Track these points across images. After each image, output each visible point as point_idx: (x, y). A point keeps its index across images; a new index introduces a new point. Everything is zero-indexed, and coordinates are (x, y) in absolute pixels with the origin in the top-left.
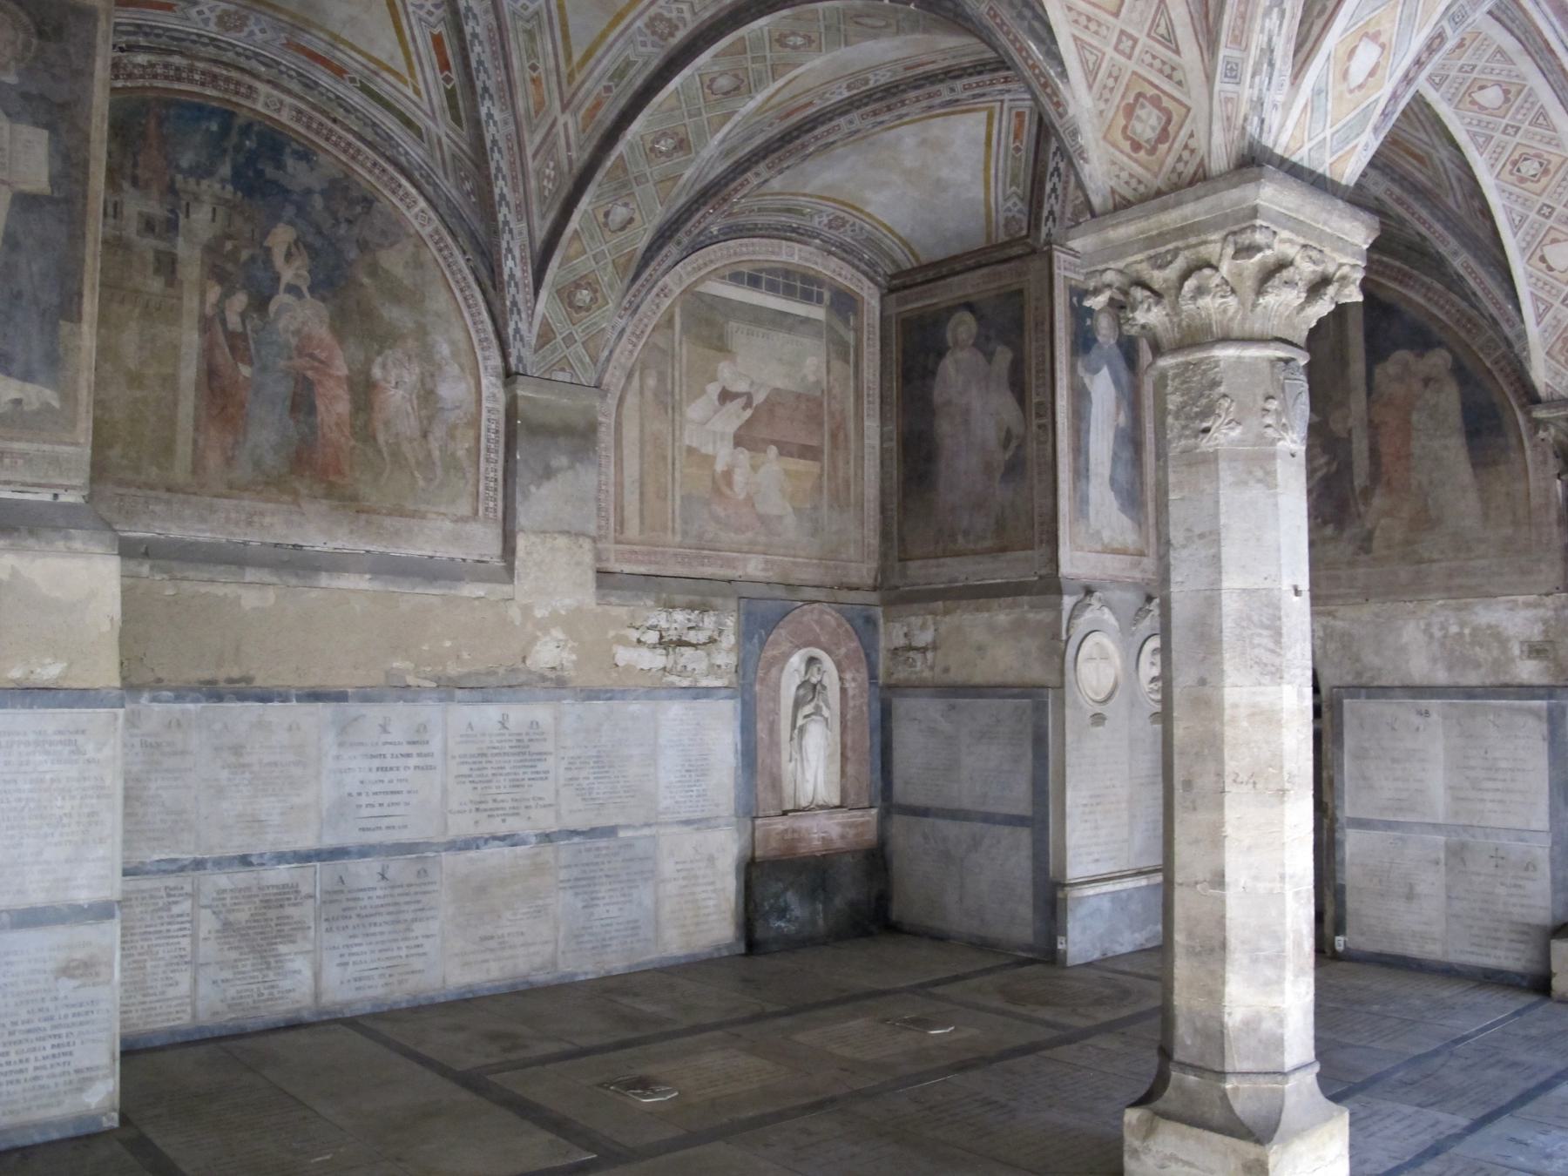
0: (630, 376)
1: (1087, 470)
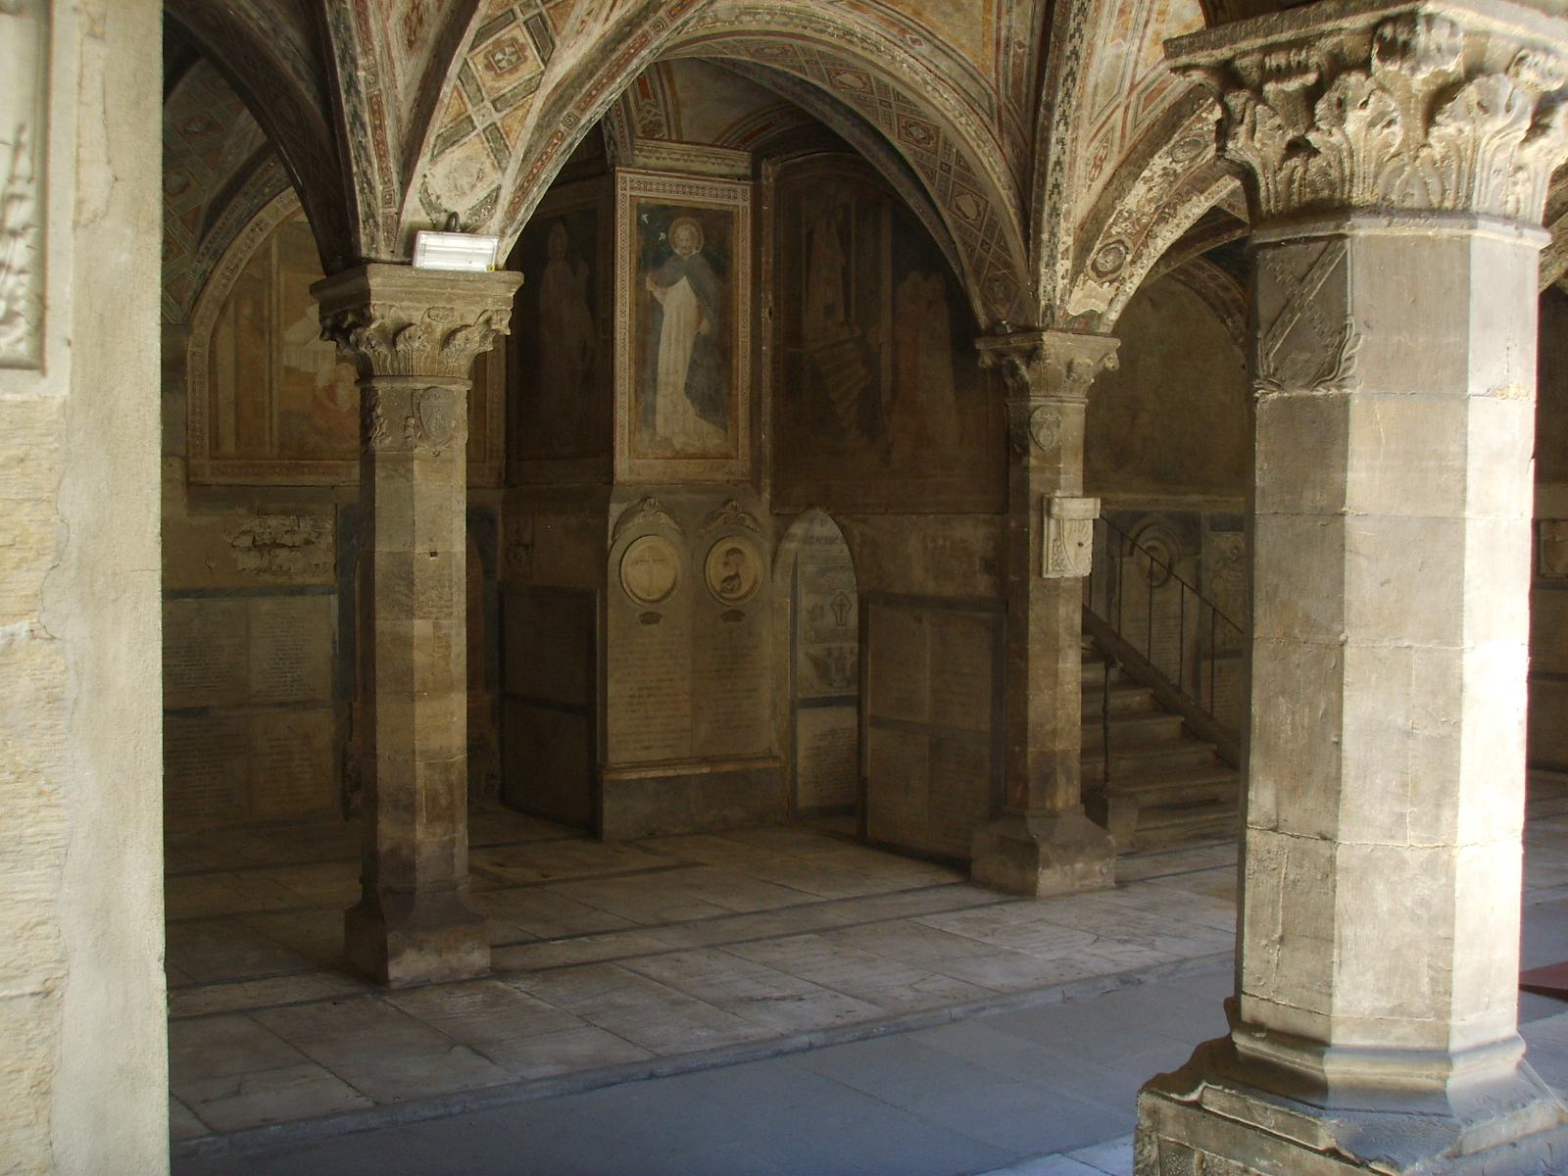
0: (223, 309)
1: (655, 380)
